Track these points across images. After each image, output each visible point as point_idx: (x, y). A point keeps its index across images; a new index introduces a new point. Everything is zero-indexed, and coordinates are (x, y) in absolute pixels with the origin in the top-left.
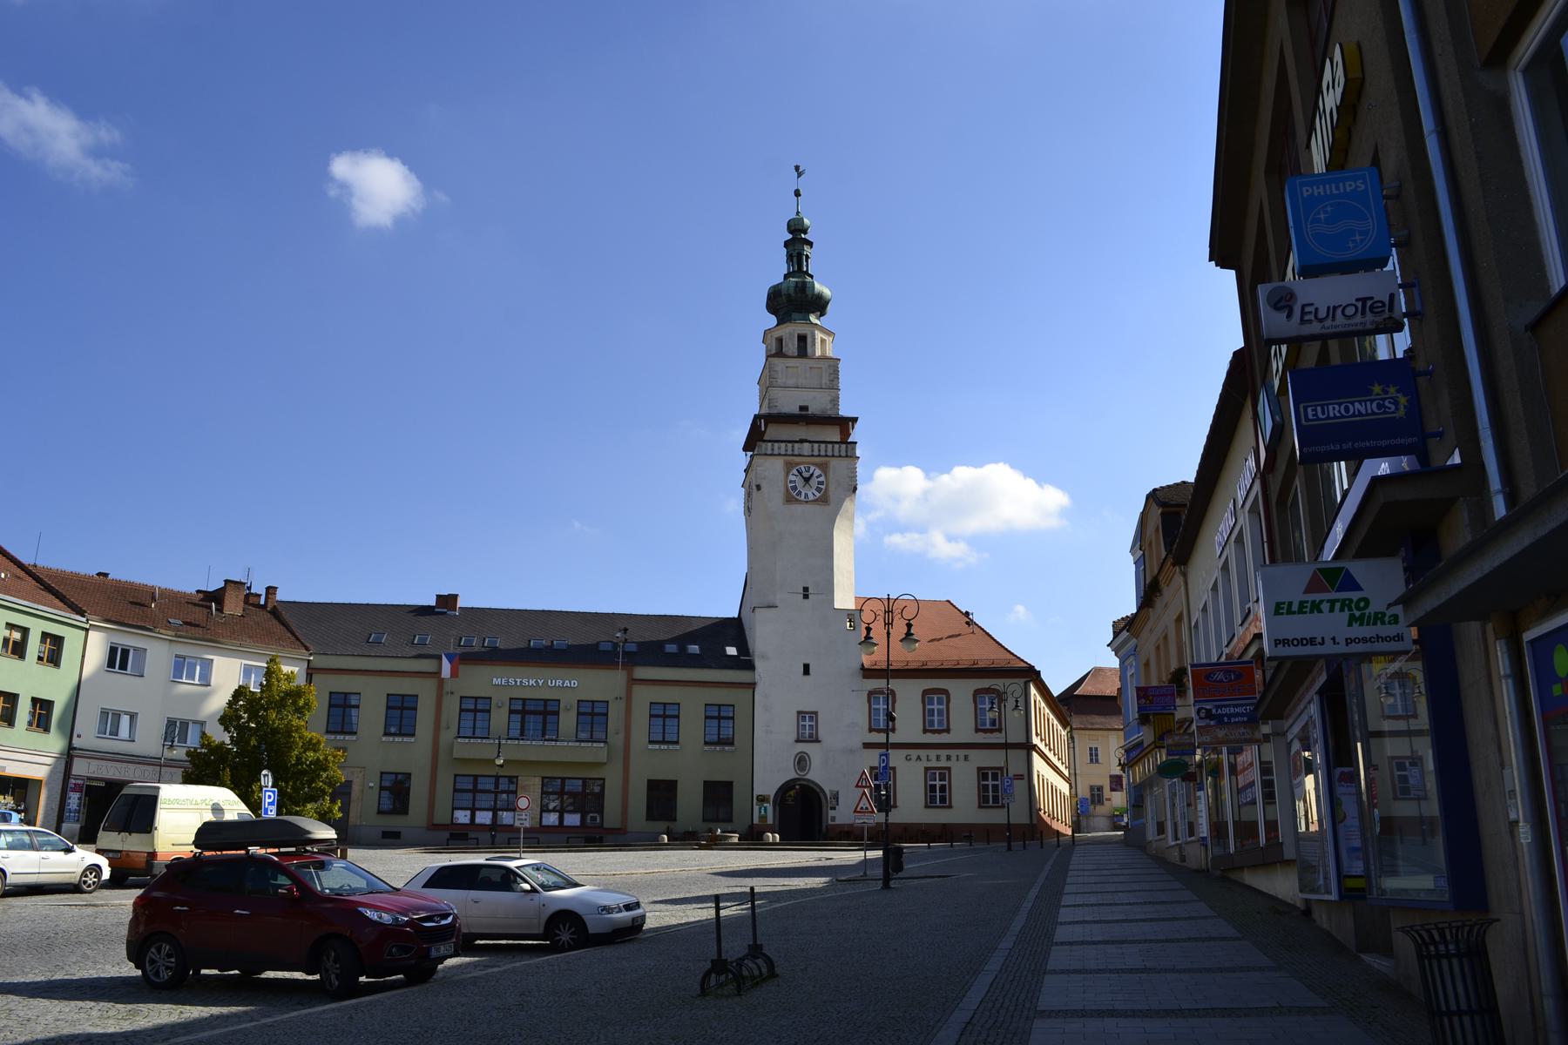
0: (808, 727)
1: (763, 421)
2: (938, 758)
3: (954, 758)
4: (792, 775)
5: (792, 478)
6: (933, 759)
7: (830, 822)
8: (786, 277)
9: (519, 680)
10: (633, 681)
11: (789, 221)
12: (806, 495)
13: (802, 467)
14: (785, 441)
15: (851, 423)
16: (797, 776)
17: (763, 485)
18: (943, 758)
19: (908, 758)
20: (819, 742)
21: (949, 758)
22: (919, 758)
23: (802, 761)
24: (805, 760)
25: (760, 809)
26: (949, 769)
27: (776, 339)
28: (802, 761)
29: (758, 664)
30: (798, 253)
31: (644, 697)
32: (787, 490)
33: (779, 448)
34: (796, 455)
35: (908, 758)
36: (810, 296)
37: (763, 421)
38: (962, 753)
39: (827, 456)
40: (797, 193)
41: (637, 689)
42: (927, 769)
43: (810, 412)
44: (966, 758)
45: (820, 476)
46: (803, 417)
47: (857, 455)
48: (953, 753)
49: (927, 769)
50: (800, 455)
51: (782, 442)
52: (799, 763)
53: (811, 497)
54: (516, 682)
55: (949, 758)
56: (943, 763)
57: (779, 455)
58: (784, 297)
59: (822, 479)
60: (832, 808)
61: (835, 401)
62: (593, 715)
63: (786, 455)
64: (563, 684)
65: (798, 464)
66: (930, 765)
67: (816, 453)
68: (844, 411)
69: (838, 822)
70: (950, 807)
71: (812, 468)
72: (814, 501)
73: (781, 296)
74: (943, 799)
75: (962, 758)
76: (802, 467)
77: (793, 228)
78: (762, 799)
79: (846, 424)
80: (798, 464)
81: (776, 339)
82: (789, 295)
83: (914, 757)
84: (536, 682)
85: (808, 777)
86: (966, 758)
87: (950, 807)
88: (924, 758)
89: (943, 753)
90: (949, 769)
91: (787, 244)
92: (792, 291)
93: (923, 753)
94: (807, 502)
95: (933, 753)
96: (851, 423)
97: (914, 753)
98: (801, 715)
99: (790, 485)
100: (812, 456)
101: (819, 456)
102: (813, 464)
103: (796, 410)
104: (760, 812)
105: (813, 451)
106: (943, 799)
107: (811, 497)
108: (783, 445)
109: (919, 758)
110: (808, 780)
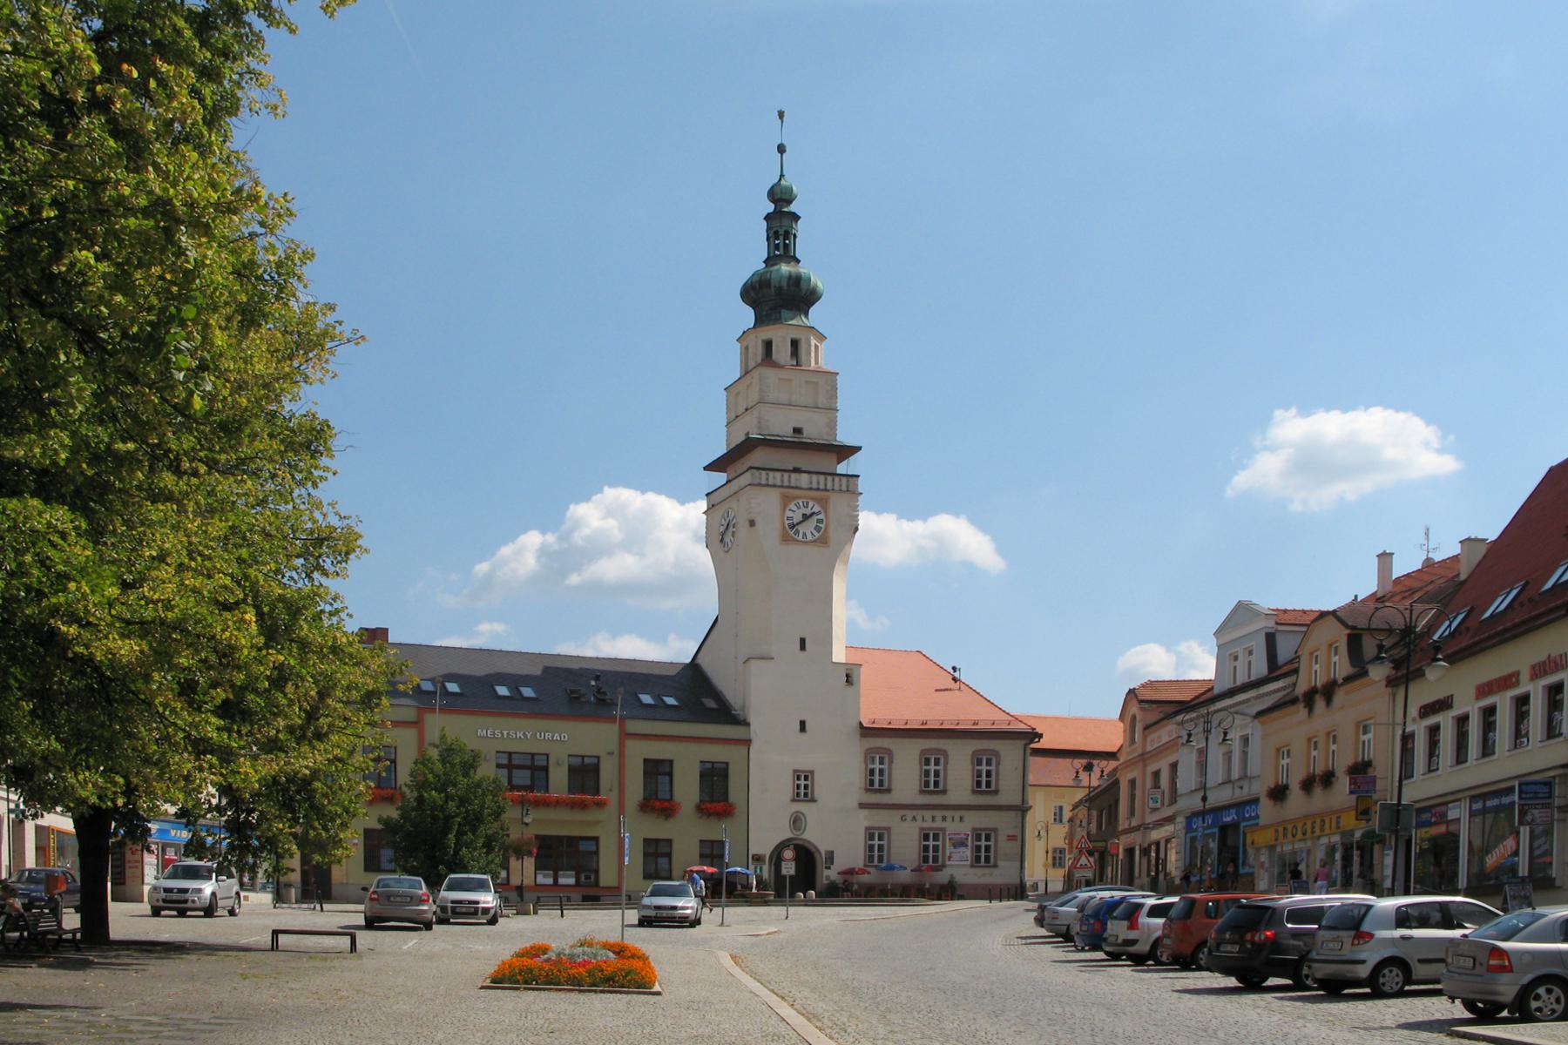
0: (804, 787)
2: (933, 819)
3: (949, 819)
4: (789, 835)
6: (928, 821)
8: (770, 261)
9: (505, 733)
10: (625, 735)
11: (773, 187)
12: (805, 534)
17: (758, 521)
18: (939, 819)
19: (903, 819)
22: (914, 819)
23: (797, 821)
25: (756, 868)
27: (763, 341)
28: (797, 821)
31: (638, 752)
32: (784, 527)
33: (774, 478)
34: (792, 488)
36: (804, 292)
38: (957, 814)
39: (826, 490)
40: (781, 149)
41: (631, 744)
42: (922, 829)
44: (961, 819)
45: (819, 513)
46: (797, 443)
47: (860, 491)
48: (948, 814)
49: (922, 829)
50: (797, 488)
52: (794, 822)
53: (810, 537)
54: (503, 734)
55: (944, 819)
56: (939, 824)
57: (774, 486)
60: (826, 868)
61: (833, 425)
62: (585, 774)
63: (782, 486)
64: (553, 737)
65: (795, 498)
66: (925, 825)
67: (822, 486)
68: (844, 437)
72: (815, 541)
74: (987, 859)
75: (957, 819)
77: (778, 196)
78: (758, 859)
79: (846, 452)
81: (763, 341)
82: (780, 288)
84: (524, 734)
86: (961, 819)
88: (919, 818)
89: (939, 814)
91: (768, 218)
92: (784, 284)
93: (919, 814)
95: (928, 814)
97: (909, 814)
98: (797, 775)
100: (811, 489)
101: (818, 489)
102: (813, 499)
105: (811, 483)
106: (987, 859)
107: (810, 537)
109: (914, 819)
110: (805, 840)
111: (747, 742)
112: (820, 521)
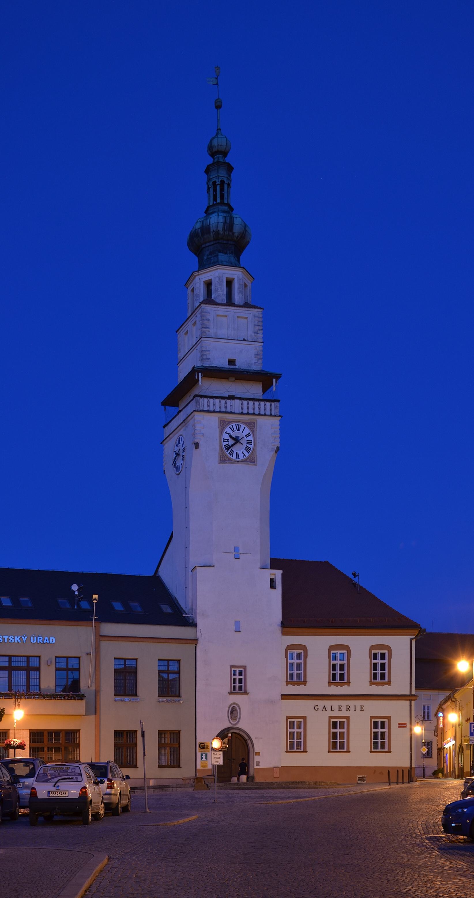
1: (200, 374)
2: (340, 708)
3: (352, 708)
4: (228, 725)
7: (256, 767)
12: (237, 454)
13: (234, 425)
14: (216, 397)
15: (274, 380)
16: (230, 725)
17: (201, 443)
18: (344, 708)
20: (248, 693)
21: (348, 708)
23: (234, 712)
24: (236, 710)
25: (202, 755)
26: (348, 718)
29: (199, 621)
30: (221, 181)
33: (214, 405)
34: (228, 413)
35: (316, 708)
37: (200, 374)
38: (358, 703)
39: (254, 414)
42: (330, 718)
43: (237, 367)
44: (361, 708)
48: (351, 703)
49: (330, 718)
50: (231, 413)
51: (216, 397)
52: (232, 713)
53: (241, 457)
55: (348, 708)
56: (344, 713)
57: (214, 412)
59: (250, 438)
63: (220, 412)
65: (230, 422)
69: (261, 766)
70: (348, 752)
73: (209, 233)
75: (358, 708)
76: (234, 425)
80: (230, 422)
83: (321, 708)
85: (238, 726)
86: (361, 708)
87: (348, 752)
88: (328, 708)
89: (344, 703)
90: (348, 718)
93: (327, 703)
94: (238, 462)
95: (336, 703)
96: (274, 380)
97: (321, 703)
100: (242, 413)
101: (248, 414)
102: (245, 423)
103: (225, 365)
104: (202, 758)
105: (242, 409)
107: (241, 457)
108: (217, 401)
110: (239, 729)
111: (195, 641)
112: (249, 442)
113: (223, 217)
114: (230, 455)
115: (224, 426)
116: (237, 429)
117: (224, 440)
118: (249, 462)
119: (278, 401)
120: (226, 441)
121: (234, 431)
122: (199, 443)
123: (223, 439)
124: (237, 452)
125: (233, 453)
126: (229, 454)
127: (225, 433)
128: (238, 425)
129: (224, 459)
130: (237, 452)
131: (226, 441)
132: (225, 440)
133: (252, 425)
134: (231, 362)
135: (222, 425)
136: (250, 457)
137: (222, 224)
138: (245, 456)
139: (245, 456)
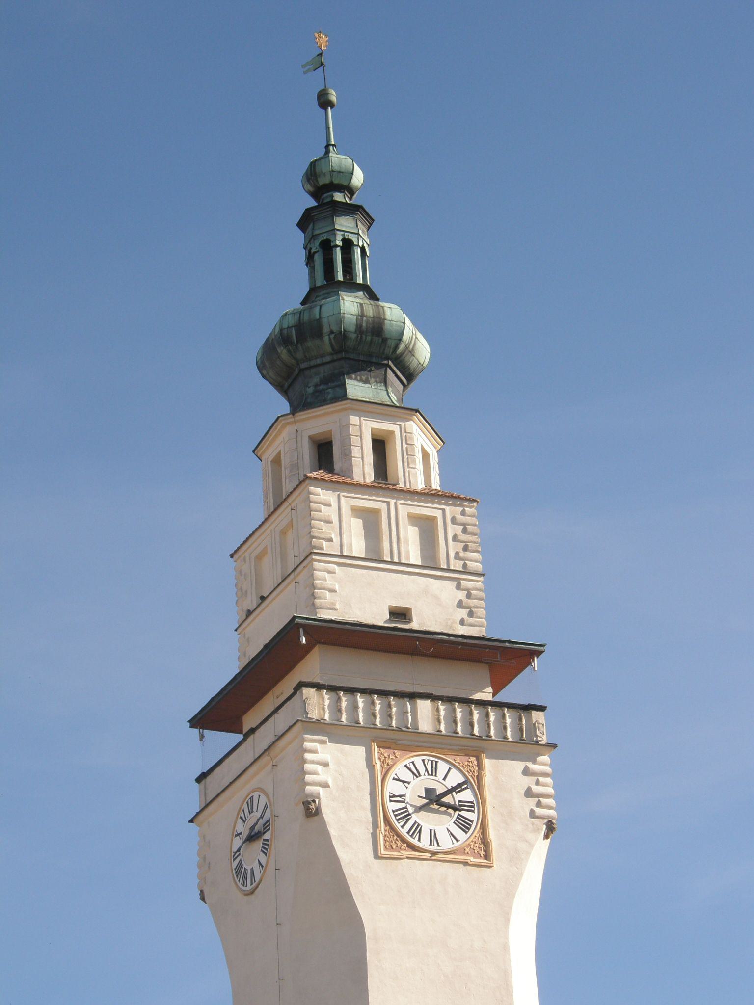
5: (392, 787)
12: (433, 837)
27: (312, 439)
53: (446, 843)
58: (326, 339)
71: (443, 767)
81: (312, 439)
94: (434, 854)
99: (391, 807)
107: (446, 843)
113: (355, 304)
114: (411, 836)
115: (390, 762)
116: (427, 770)
117: (390, 797)
118: (470, 856)
119: (542, 708)
120: (398, 799)
121: (420, 776)
122: (317, 801)
123: (388, 795)
124: (431, 830)
125: (420, 832)
126: (408, 833)
127: (394, 779)
128: (430, 762)
129: (394, 846)
130: (433, 828)
131: (398, 799)
132: (395, 796)
133: (471, 764)
134: (400, 614)
135: (383, 758)
136: (472, 844)
137: (355, 317)
138: (457, 840)
139: (457, 840)
